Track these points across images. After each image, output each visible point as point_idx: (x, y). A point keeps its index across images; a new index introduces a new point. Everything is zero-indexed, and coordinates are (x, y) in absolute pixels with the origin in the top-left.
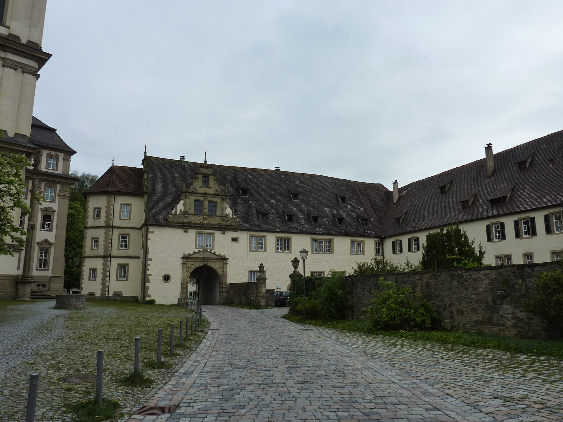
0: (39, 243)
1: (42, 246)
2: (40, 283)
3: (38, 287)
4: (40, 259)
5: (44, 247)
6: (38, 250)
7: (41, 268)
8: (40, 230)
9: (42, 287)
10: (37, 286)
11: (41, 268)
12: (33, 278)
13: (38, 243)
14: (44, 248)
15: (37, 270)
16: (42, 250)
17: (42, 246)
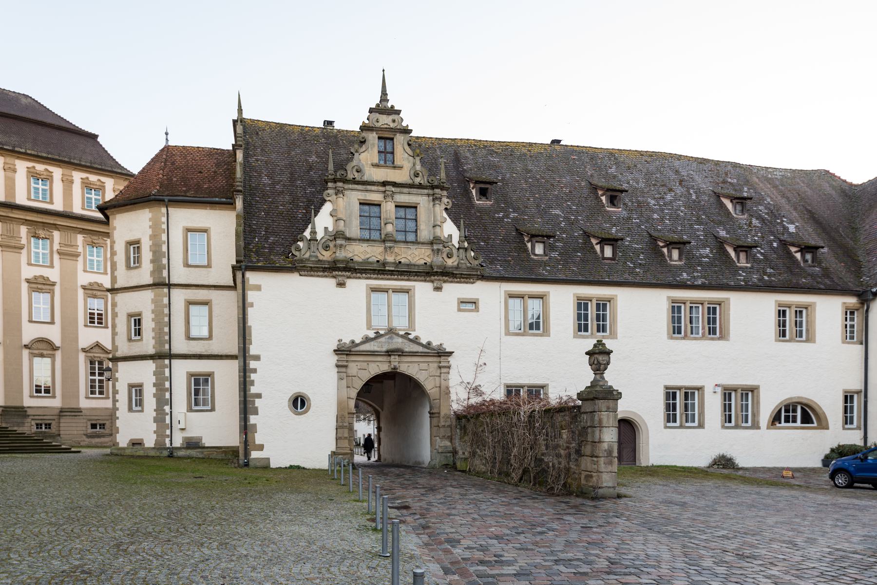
0: (85, 349)
1: (92, 355)
2: (94, 422)
3: (92, 428)
4: (91, 379)
5: (95, 357)
6: (85, 362)
7: (95, 394)
8: (86, 326)
9: (100, 428)
10: (89, 427)
11: (95, 394)
12: (81, 412)
13: (84, 350)
14: (96, 359)
15: (87, 398)
16: (92, 363)
17: (92, 355)
